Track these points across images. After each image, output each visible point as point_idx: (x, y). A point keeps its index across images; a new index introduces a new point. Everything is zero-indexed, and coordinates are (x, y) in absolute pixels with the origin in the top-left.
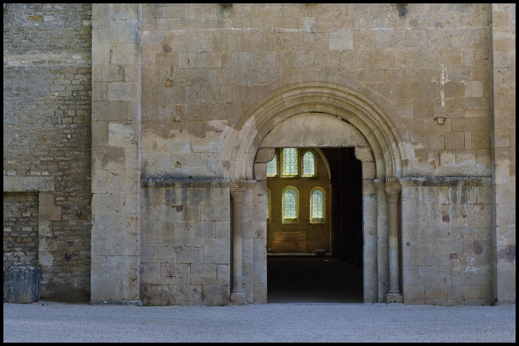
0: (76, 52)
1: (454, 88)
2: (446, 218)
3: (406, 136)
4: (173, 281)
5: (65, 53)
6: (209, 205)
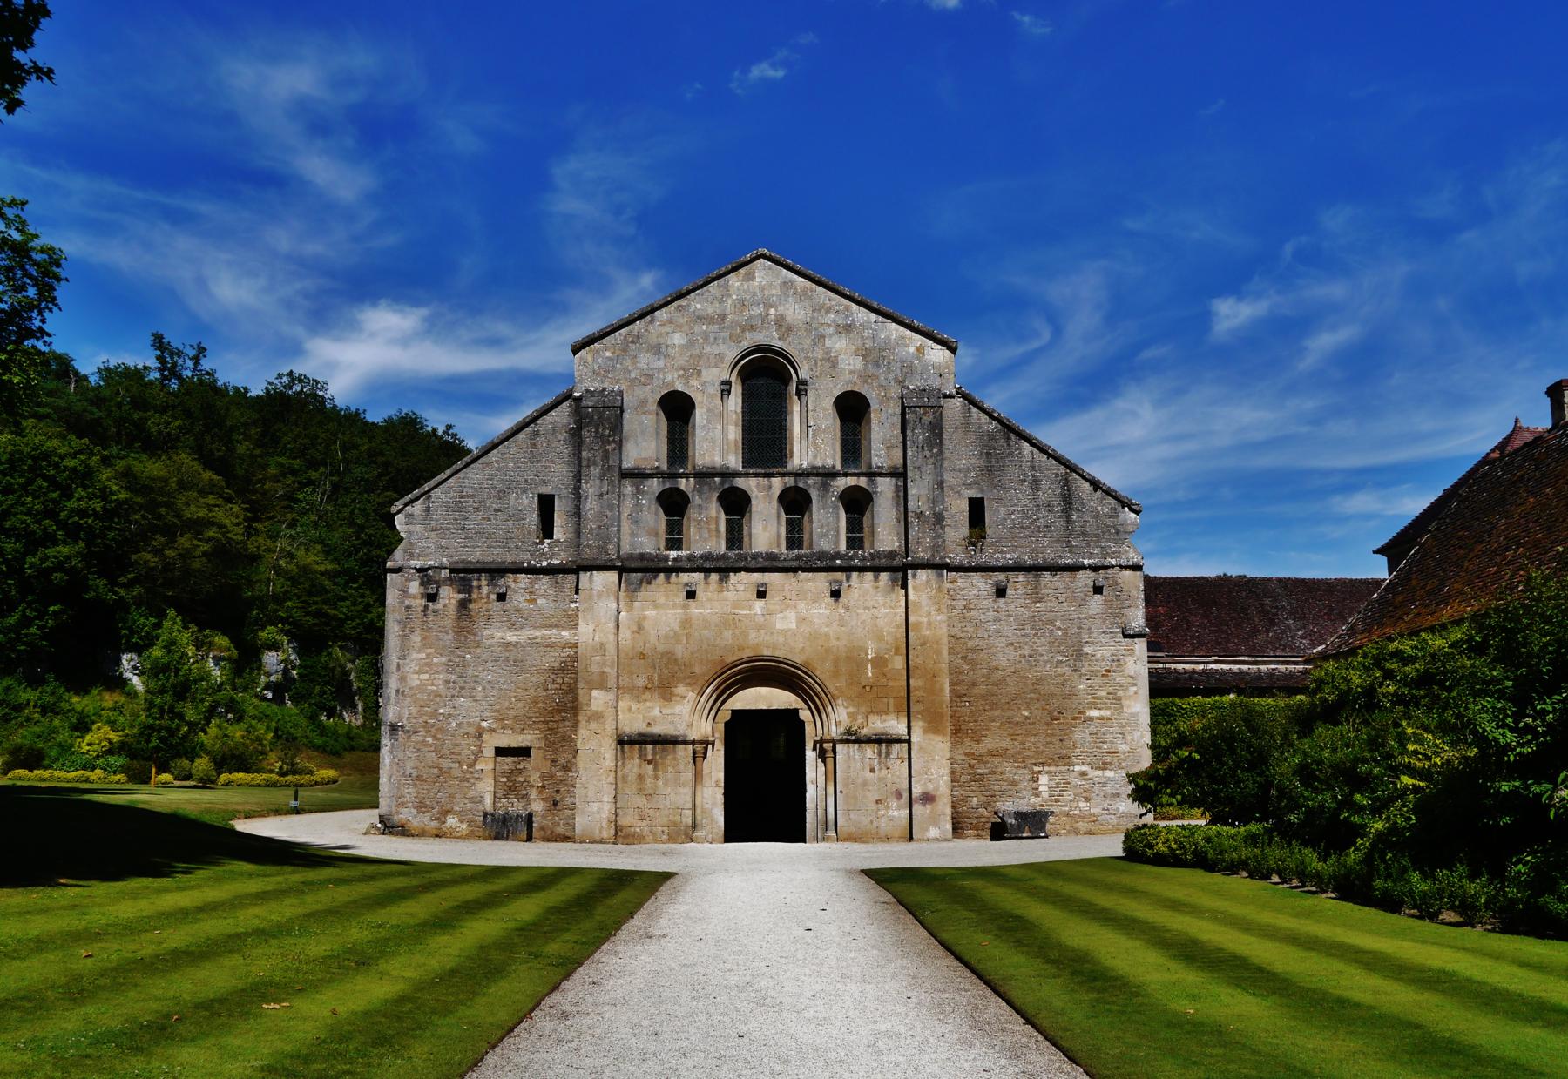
0: (564, 629)
1: (879, 662)
2: (873, 770)
3: (840, 701)
4: (644, 823)
5: (554, 631)
6: (674, 759)
